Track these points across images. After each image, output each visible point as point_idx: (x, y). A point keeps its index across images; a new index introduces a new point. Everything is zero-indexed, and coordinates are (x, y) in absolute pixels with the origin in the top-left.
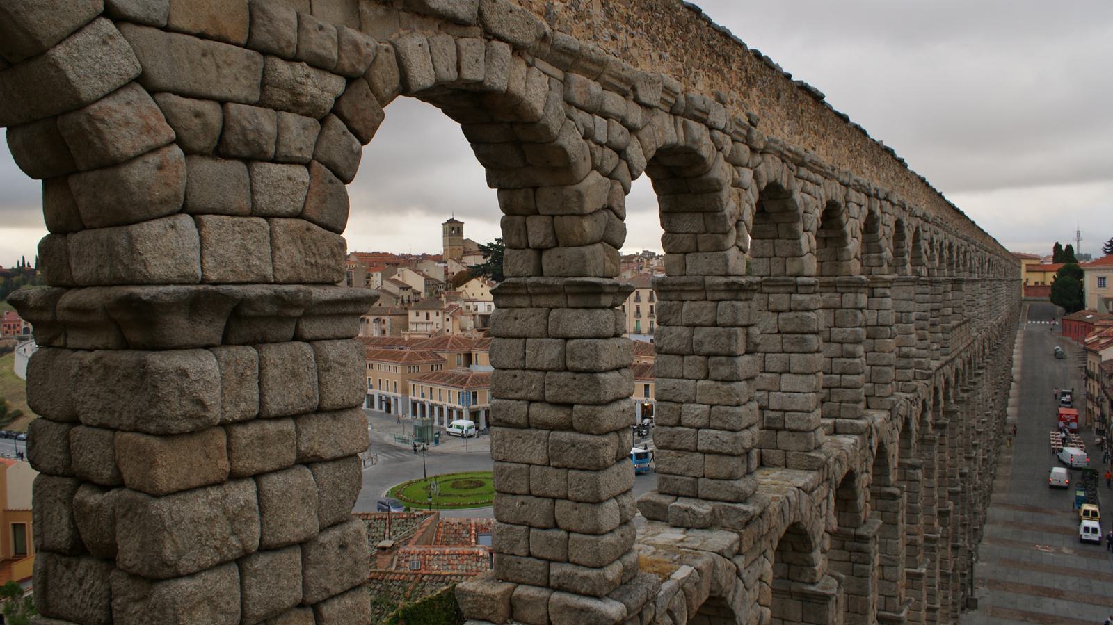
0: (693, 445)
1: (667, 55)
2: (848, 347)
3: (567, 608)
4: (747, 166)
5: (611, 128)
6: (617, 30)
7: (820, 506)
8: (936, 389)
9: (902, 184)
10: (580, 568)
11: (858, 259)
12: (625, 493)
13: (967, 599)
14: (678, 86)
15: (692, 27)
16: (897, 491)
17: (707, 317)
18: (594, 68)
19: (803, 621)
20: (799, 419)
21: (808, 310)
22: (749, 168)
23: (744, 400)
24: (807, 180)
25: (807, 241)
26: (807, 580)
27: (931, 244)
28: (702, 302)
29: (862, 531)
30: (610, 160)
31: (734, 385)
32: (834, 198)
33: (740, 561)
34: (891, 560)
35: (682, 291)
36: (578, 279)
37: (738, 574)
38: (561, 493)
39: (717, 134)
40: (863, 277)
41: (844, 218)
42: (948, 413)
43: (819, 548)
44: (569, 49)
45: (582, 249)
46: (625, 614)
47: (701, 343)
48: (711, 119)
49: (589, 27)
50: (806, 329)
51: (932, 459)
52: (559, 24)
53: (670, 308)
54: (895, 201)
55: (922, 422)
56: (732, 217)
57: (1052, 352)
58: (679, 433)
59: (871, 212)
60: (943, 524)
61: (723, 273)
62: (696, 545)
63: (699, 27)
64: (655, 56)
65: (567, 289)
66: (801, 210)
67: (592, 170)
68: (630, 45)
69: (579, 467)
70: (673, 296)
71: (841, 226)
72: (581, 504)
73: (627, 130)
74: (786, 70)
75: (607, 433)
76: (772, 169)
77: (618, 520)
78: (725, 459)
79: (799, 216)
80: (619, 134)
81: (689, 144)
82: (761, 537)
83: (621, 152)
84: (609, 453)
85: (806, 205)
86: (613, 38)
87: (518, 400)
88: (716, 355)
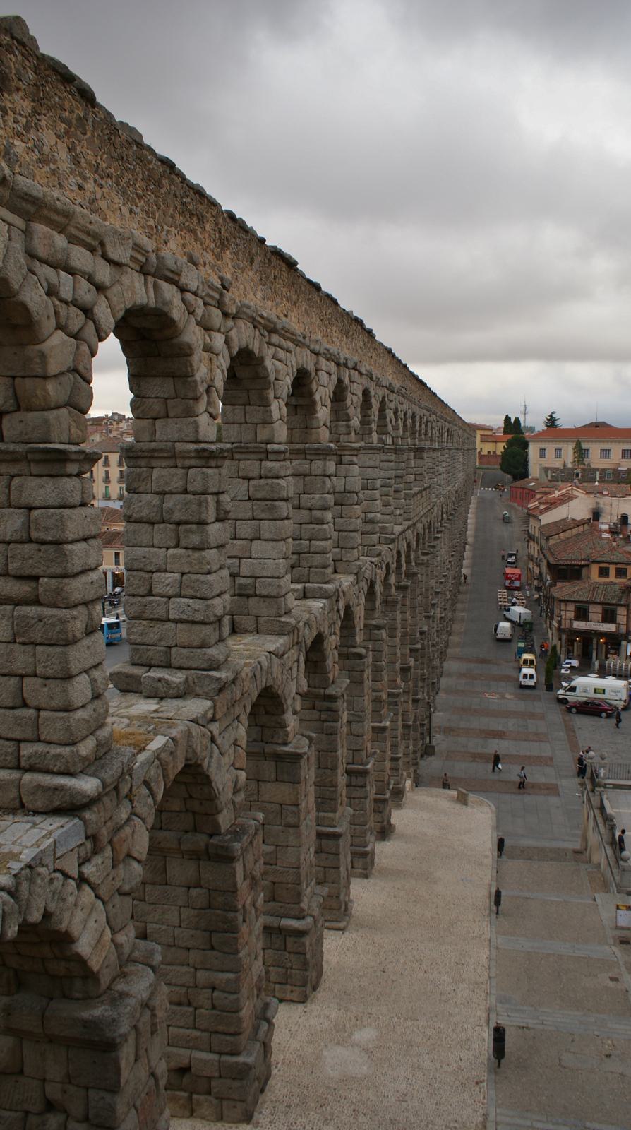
0: (165, 615)
1: (138, 210)
2: (317, 513)
3: (39, 787)
4: (219, 331)
5: (77, 285)
6: (85, 179)
7: (291, 669)
8: (399, 553)
9: (370, 354)
10: (52, 746)
11: (327, 427)
12: (96, 666)
13: (426, 747)
14: (149, 245)
15: (165, 182)
16: (363, 651)
17: (177, 484)
18: (60, 219)
19: (277, 780)
20: (270, 585)
21: (278, 478)
22: (221, 332)
23: (215, 568)
25: (278, 408)
26: (280, 741)
27: (396, 413)
28: (172, 469)
30: (76, 319)
31: (205, 553)
32: (305, 366)
33: (214, 727)
34: (359, 716)
35: (152, 457)
36: (41, 446)
37: (213, 740)
38: (29, 670)
39: (189, 296)
40: (332, 445)
41: (314, 386)
42: (410, 575)
43: (291, 709)
44: (30, 196)
45: (46, 413)
46: (101, 789)
47: (171, 511)
48: (183, 280)
49: (54, 172)
50: (276, 496)
52: (20, 166)
53: (140, 475)
54: (363, 371)
55: (386, 585)
56: (202, 382)
57: (501, 517)
58: (150, 603)
59: (340, 381)
60: (405, 680)
61: (193, 439)
62: (171, 715)
63: (172, 183)
64: (125, 210)
65: (29, 456)
66: (272, 377)
67: (56, 329)
68: (99, 196)
69: (46, 642)
70: (143, 462)
71: (311, 394)
72: (51, 680)
73: (93, 288)
74: (260, 234)
75: (76, 606)
76: (244, 335)
77: (89, 694)
78: (197, 627)
79: (270, 383)
80: (85, 292)
81: (160, 305)
82: (234, 703)
83: (87, 312)
84: (78, 626)
85: (277, 372)
86: (80, 187)
88: (187, 523)
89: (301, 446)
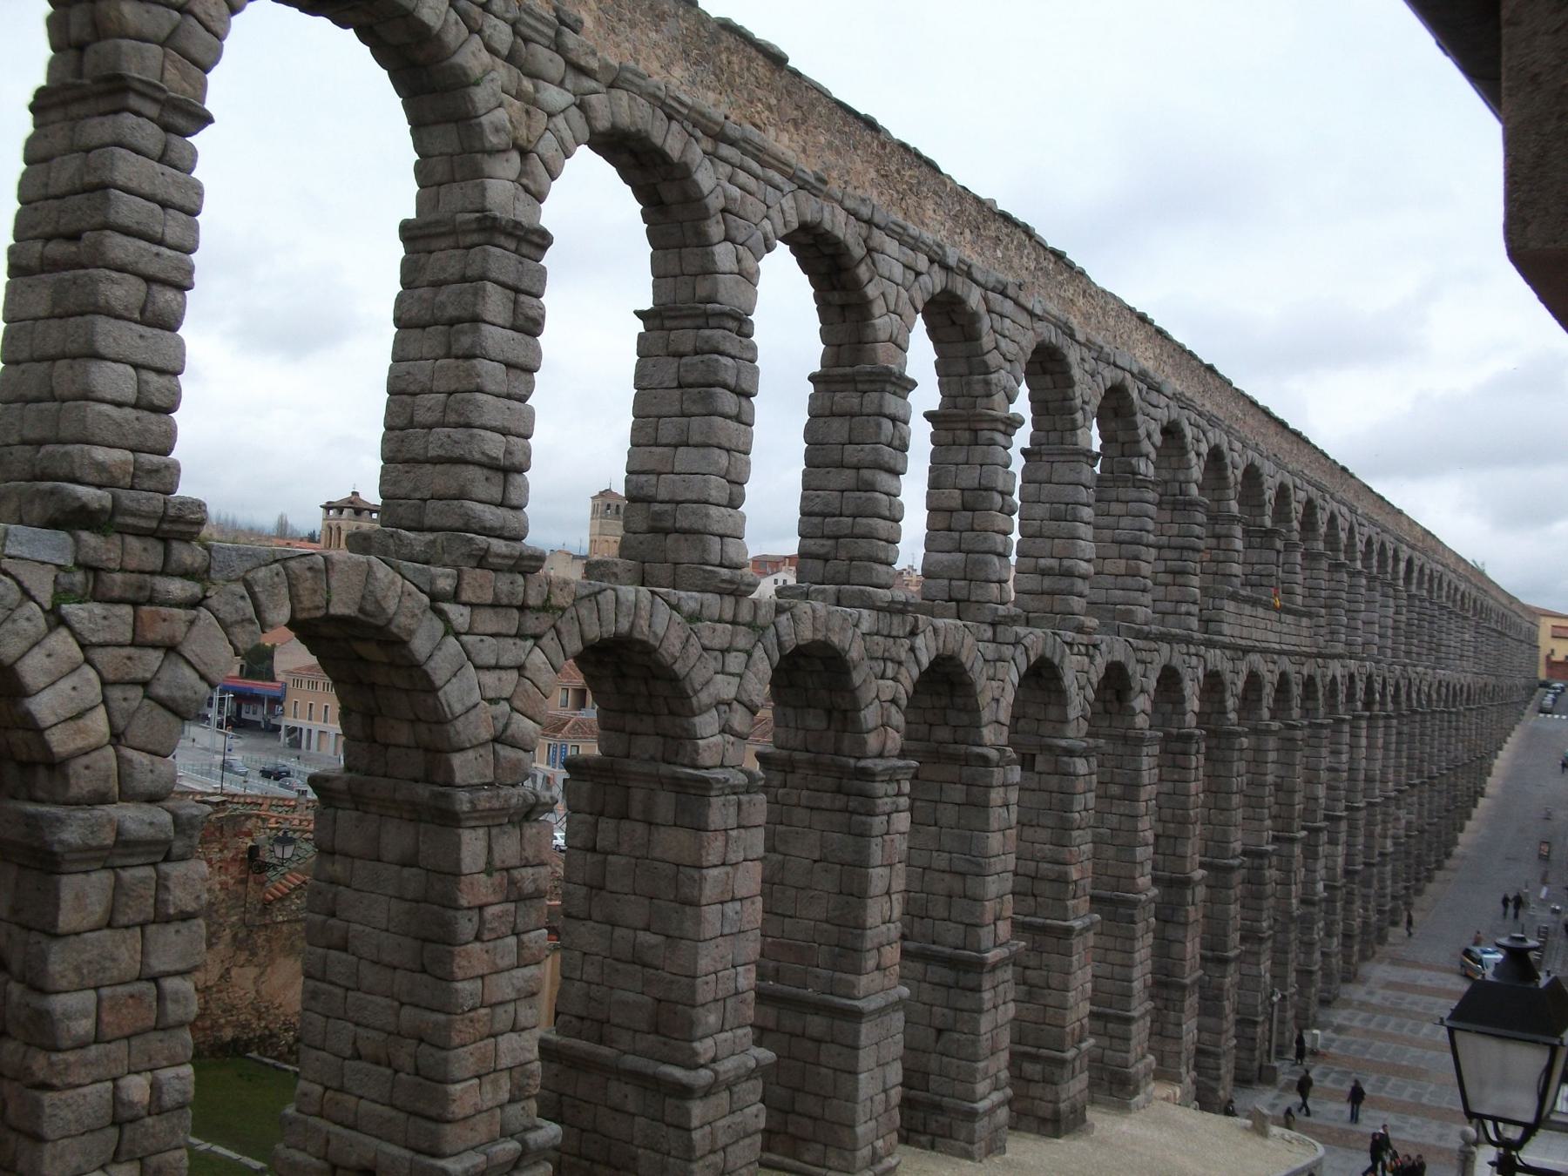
4: (561, 84)
13: (1261, 1067)
16: (993, 754)
17: (454, 269)
21: (722, 353)
24: (741, 168)
26: (686, 761)
32: (827, 226)
41: (863, 272)
47: (443, 305)
50: (712, 379)
51: (1138, 770)
66: (715, 203)
71: (858, 286)
88: (460, 320)
89: (848, 370)
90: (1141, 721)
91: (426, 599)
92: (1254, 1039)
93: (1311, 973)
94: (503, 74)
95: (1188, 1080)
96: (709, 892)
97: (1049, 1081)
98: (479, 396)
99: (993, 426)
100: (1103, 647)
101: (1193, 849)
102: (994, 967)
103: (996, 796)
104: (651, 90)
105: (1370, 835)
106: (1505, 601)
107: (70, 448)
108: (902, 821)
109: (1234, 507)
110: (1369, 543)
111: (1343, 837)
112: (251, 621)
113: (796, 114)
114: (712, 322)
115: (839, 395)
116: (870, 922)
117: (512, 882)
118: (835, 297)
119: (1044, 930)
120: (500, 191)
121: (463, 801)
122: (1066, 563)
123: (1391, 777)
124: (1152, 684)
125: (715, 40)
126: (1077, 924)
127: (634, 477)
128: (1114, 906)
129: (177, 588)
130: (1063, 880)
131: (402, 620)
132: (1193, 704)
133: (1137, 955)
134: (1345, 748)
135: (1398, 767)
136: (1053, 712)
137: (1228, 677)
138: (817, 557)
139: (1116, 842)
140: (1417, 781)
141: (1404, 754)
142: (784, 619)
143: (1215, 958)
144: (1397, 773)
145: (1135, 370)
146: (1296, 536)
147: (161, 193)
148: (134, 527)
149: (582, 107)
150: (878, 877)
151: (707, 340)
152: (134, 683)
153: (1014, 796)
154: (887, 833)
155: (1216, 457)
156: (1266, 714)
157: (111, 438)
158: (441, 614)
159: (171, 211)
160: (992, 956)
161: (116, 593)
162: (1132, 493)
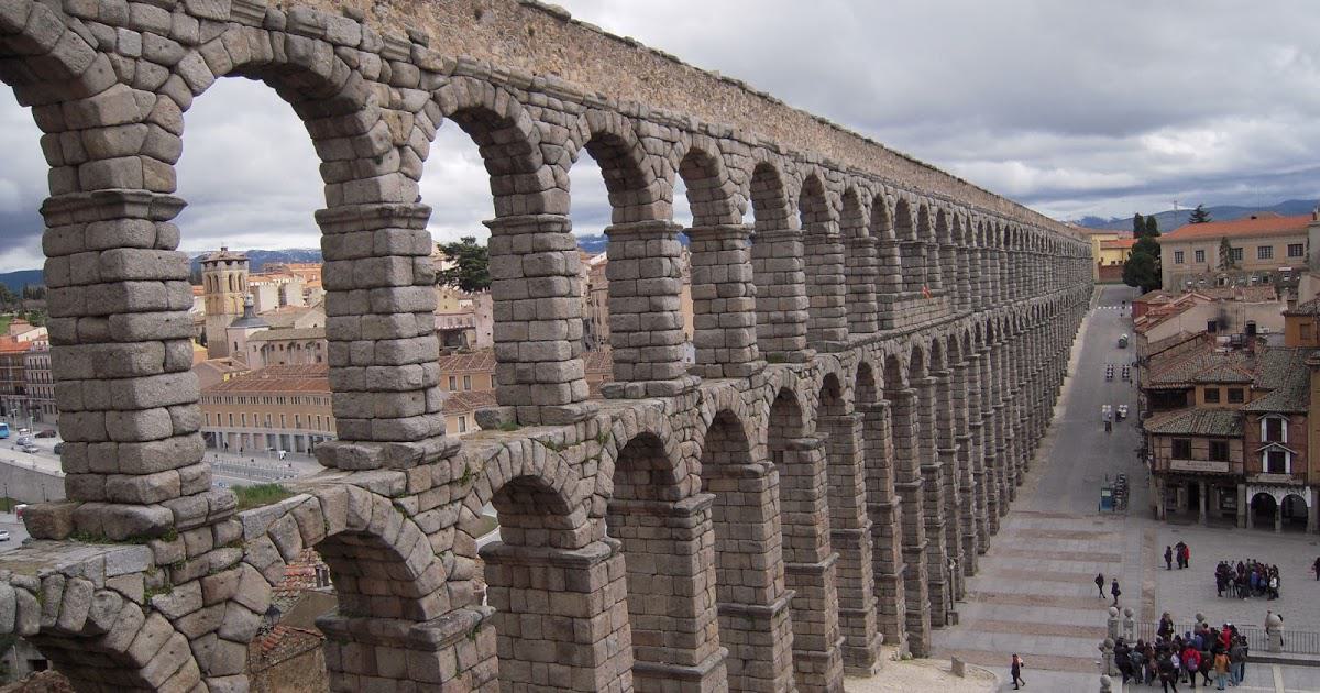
3: (115, 515)
4: (419, 87)
12: (185, 404)
16: (760, 468)
17: (364, 248)
20: (549, 370)
21: (552, 250)
24: (549, 107)
29: (682, 505)
31: (392, 317)
32: (610, 130)
41: (637, 155)
48: (331, 34)
50: (548, 271)
66: (534, 141)
67: (118, 82)
81: (293, 60)
83: (172, 68)
87: (68, 317)
88: (375, 287)
89: (634, 225)
90: (849, 408)
91: (388, 502)
92: (941, 597)
93: (971, 538)
94: (378, 93)
95: (903, 640)
96: (597, 633)
97: (817, 673)
98: (401, 342)
99: (734, 235)
100: (820, 367)
101: (890, 485)
102: (777, 614)
103: (765, 498)
104: (481, 70)
105: (999, 430)
106: (1069, 234)
107: (133, 480)
108: (710, 538)
109: (892, 233)
110: (980, 225)
111: (983, 439)
112: (279, 561)
113: (581, 52)
114: (542, 228)
115: (628, 245)
116: (697, 612)
117: (475, 676)
118: (617, 174)
119: (804, 571)
120: (389, 182)
121: (436, 634)
122: (790, 314)
123: (1008, 385)
124: (853, 379)
125: (518, 15)
126: (825, 564)
127: (500, 345)
128: (844, 540)
129: (226, 556)
130: (813, 536)
131: (377, 523)
132: (880, 383)
133: (863, 570)
134: (978, 377)
135: (1012, 375)
136: (792, 421)
137: (900, 356)
138: (627, 362)
139: (842, 495)
140: (1024, 383)
141: (1015, 366)
142: (617, 425)
143: (911, 551)
144: (1012, 381)
145: (821, 162)
146: (933, 239)
147: (162, 273)
148: (190, 526)
149: (435, 99)
150: (699, 580)
151: (543, 242)
152: (210, 633)
153: (776, 493)
154: (701, 549)
155: (878, 201)
156: (926, 372)
157: (161, 466)
158: (398, 507)
159: (170, 283)
160: (775, 607)
161: (187, 578)
162: (826, 248)
